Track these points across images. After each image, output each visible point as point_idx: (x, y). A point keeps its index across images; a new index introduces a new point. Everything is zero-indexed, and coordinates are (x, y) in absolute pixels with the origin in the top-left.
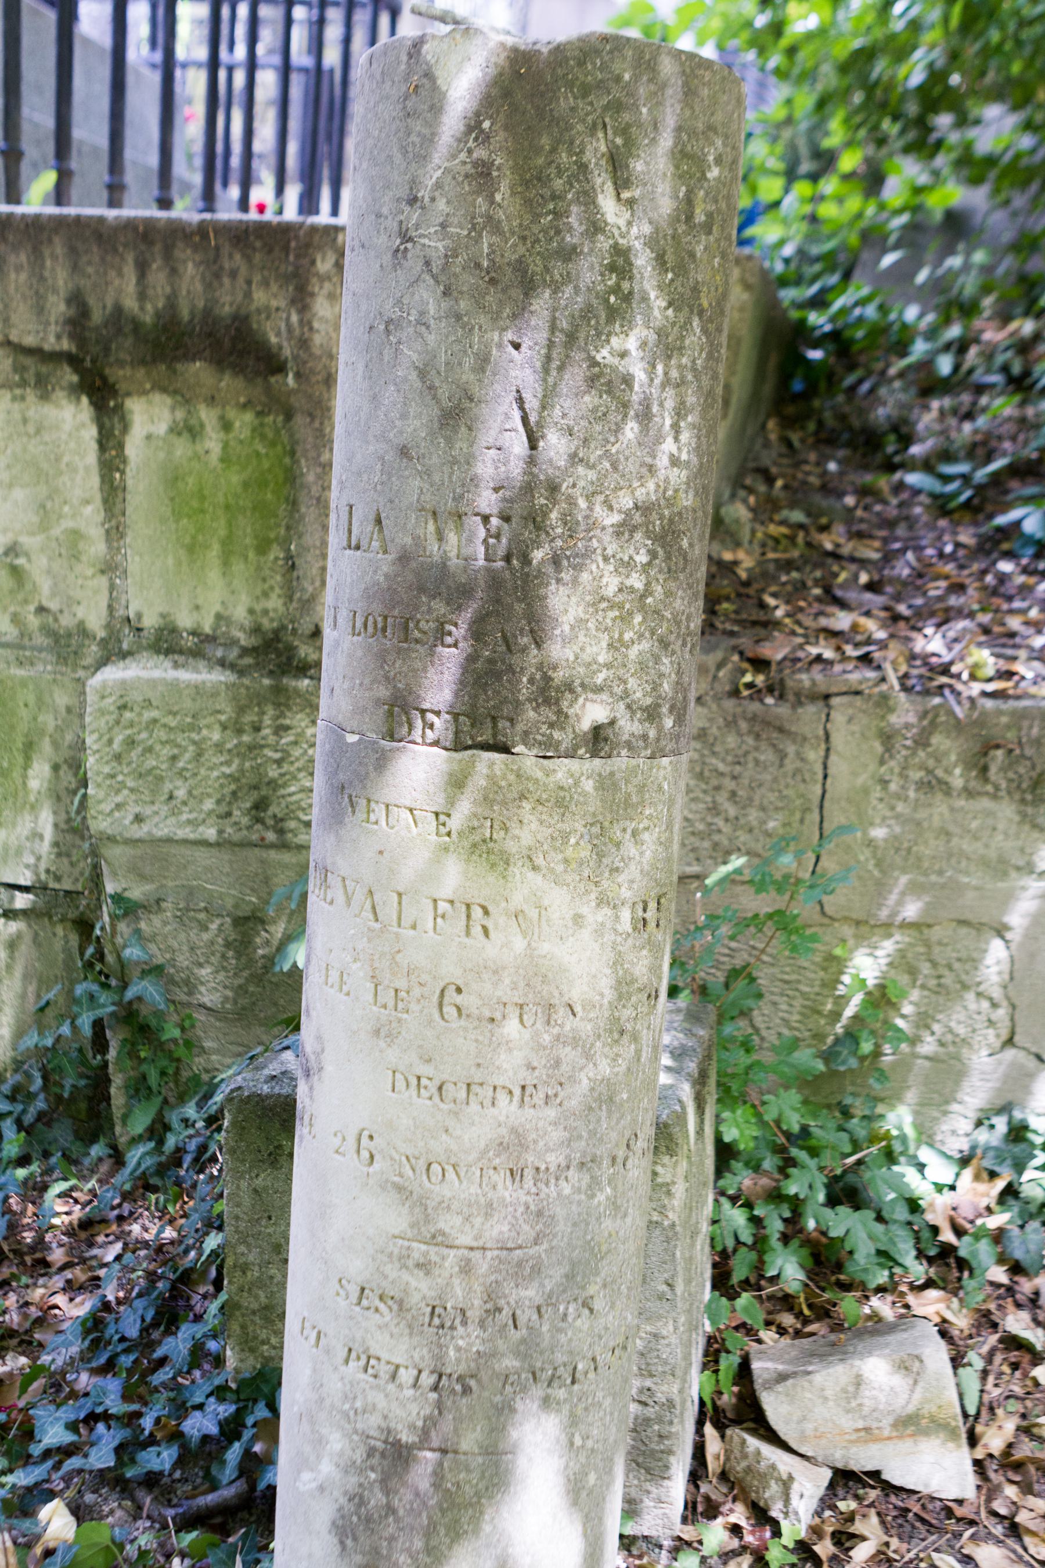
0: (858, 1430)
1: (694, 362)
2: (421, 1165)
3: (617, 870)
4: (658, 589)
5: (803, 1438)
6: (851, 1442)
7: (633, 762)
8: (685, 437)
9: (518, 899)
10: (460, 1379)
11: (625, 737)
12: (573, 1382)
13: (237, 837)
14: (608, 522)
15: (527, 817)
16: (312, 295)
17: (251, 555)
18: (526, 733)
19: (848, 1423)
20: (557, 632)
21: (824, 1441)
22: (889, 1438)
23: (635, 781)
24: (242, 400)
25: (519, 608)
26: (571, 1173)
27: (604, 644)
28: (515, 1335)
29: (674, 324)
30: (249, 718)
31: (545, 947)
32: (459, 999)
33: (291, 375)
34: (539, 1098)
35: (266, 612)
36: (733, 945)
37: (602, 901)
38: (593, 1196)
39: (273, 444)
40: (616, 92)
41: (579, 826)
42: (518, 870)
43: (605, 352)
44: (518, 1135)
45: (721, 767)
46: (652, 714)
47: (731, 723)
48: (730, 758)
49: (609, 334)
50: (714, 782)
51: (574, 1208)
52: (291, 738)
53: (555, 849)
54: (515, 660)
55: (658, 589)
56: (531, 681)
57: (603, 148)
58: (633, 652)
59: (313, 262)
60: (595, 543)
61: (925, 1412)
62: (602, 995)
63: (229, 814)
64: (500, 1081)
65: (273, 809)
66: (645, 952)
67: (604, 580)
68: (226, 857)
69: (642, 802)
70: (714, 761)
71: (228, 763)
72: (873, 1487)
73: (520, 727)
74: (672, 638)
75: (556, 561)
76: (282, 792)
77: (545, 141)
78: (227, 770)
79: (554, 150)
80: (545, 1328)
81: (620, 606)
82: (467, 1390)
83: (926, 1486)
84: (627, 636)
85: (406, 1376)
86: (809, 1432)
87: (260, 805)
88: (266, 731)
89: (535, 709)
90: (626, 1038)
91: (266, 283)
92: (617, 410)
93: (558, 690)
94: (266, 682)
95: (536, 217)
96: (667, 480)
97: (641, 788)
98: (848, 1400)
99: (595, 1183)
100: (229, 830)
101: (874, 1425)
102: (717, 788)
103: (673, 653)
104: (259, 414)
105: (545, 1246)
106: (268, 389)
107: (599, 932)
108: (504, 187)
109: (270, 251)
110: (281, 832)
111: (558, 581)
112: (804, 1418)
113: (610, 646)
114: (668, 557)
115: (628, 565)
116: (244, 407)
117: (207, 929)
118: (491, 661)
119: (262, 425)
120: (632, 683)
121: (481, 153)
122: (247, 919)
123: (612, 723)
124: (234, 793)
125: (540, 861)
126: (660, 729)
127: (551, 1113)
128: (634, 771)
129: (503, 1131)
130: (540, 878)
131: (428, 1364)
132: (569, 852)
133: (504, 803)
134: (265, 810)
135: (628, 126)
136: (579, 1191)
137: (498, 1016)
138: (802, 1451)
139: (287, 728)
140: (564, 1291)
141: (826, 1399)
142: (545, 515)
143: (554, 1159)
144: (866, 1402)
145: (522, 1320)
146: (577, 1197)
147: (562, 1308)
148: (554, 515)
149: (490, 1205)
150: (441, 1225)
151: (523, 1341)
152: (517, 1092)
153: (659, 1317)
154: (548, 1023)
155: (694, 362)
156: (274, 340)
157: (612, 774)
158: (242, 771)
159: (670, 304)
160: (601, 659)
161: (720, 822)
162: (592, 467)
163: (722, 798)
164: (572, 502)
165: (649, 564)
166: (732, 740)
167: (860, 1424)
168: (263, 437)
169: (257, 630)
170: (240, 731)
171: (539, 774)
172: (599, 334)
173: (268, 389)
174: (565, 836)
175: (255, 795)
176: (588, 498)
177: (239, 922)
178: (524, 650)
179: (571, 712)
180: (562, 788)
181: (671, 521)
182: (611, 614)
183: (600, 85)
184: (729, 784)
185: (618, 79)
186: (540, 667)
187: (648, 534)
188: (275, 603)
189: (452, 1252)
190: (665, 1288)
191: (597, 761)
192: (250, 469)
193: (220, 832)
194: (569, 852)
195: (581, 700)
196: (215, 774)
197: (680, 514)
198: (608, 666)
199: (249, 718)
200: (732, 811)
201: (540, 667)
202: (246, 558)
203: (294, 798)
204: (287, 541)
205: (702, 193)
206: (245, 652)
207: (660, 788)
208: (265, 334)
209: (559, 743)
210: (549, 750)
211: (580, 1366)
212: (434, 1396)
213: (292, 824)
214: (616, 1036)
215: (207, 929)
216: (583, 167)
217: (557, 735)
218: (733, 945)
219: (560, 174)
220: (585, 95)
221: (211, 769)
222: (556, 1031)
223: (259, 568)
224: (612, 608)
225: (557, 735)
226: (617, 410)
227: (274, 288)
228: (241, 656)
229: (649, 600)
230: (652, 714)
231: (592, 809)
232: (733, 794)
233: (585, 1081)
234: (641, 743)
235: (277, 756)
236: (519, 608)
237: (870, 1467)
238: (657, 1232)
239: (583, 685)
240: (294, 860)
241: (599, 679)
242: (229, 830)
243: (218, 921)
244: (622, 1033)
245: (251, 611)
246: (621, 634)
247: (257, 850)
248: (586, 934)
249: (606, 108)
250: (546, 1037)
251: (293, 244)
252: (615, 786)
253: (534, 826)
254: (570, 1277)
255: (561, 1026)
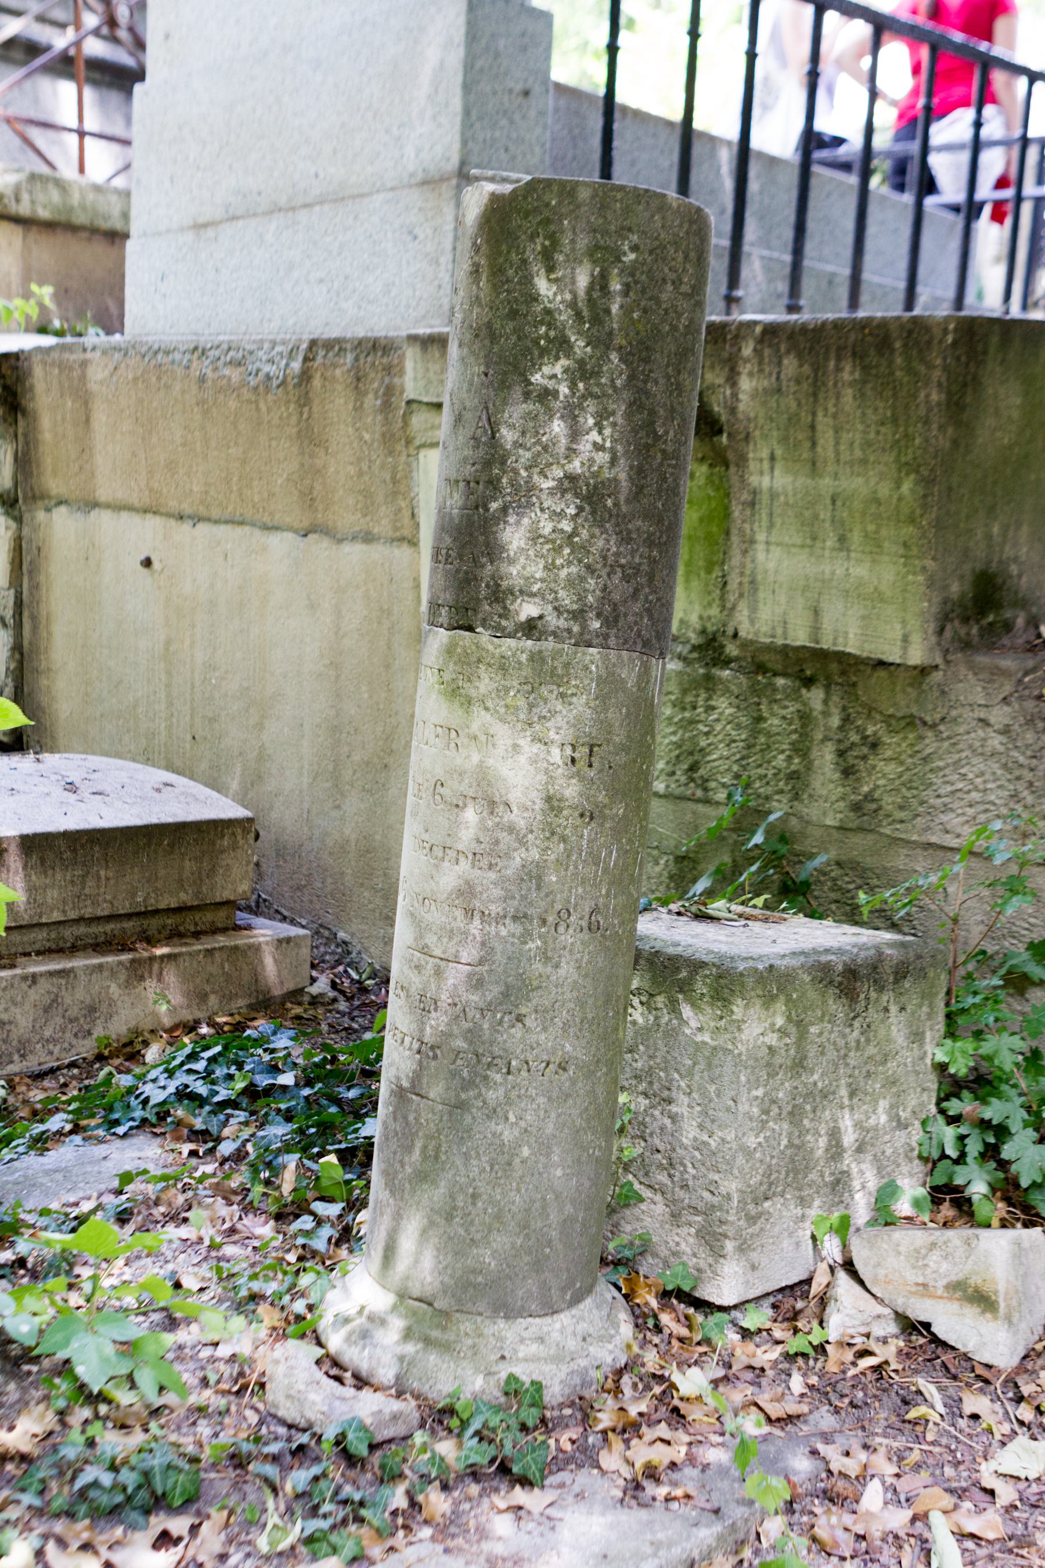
0: (917, 1284)
1: (613, 381)
2: (421, 898)
3: (545, 717)
4: (585, 533)
5: (876, 1280)
6: (911, 1292)
7: (560, 646)
8: (607, 432)
9: (475, 727)
10: (432, 1048)
11: (552, 628)
12: (509, 1073)
13: (678, 792)
14: (544, 486)
15: (483, 675)
16: (739, 374)
17: (702, 574)
18: (484, 620)
19: (912, 1276)
20: (505, 555)
21: (891, 1287)
22: (941, 1297)
23: (561, 660)
24: (700, 455)
25: (481, 538)
26: (507, 921)
27: (541, 566)
28: (466, 1025)
29: (591, 357)
30: (689, 699)
31: (491, 762)
32: (442, 790)
33: (725, 435)
34: (484, 863)
35: (709, 618)
36: (1032, 920)
37: (537, 739)
38: (526, 943)
39: (718, 489)
40: (546, 213)
41: (515, 683)
42: (477, 709)
43: (538, 376)
44: (470, 887)
45: (1021, 759)
46: (578, 615)
47: (1030, 722)
48: (1029, 753)
49: (541, 365)
50: (1017, 773)
51: (509, 946)
52: (715, 716)
53: (499, 697)
54: (478, 572)
55: (585, 533)
56: (487, 586)
57: (539, 248)
58: (563, 573)
59: (740, 349)
60: (534, 499)
61: (972, 1282)
62: (534, 803)
63: (673, 773)
64: (460, 847)
65: (702, 772)
66: (574, 781)
67: (541, 524)
68: (671, 807)
69: (568, 674)
70: (1015, 754)
71: (674, 733)
72: (924, 1336)
73: (480, 616)
74: (599, 566)
75: (504, 509)
76: (709, 758)
77: (504, 247)
78: (674, 739)
79: (509, 252)
80: (486, 1026)
81: (553, 541)
82: (435, 1057)
83: (964, 1345)
84: (559, 562)
85: (407, 1040)
86: (881, 1277)
87: (693, 768)
88: (700, 710)
89: (490, 605)
90: (556, 838)
91: (712, 367)
92: (545, 413)
93: (504, 592)
94: (702, 671)
95: (498, 296)
96: (592, 461)
97: (567, 665)
98: (917, 1259)
99: (526, 937)
100: (673, 786)
101: (931, 1283)
102: (1018, 778)
103: (599, 577)
104: (711, 466)
105: (486, 968)
106: (713, 447)
107: (533, 761)
108: (484, 278)
109: (716, 342)
110: (706, 790)
111: (505, 522)
112: (878, 1265)
113: (545, 567)
114: (593, 512)
115: (561, 515)
116: (702, 459)
117: (658, 864)
118: (466, 573)
119: (712, 474)
120: (562, 594)
121: (476, 259)
122: (684, 858)
123: (541, 617)
124: (678, 757)
125: (489, 704)
126: (584, 627)
127: (492, 875)
128: (559, 652)
129: (462, 882)
130: (489, 716)
131: (416, 1034)
132: (509, 700)
133: (469, 664)
134: (696, 771)
135: (554, 233)
136: (513, 936)
137: (461, 804)
138: (874, 1291)
139: (713, 708)
140: (501, 1004)
141: (899, 1253)
142: (499, 480)
143: (495, 909)
144: (931, 1264)
145: (470, 1015)
146: (511, 939)
147: (499, 1016)
148: (504, 480)
149: (452, 931)
150: (427, 941)
151: (470, 1031)
152: (470, 856)
153: (727, 1126)
154: (492, 813)
155: (613, 381)
156: (716, 409)
157: (540, 652)
158: (682, 740)
159: (588, 345)
160: (538, 576)
161: (1019, 808)
162: (529, 449)
163: (1021, 786)
164: (516, 472)
165: (577, 515)
166: (1030, 737)
167: (920, 1280)
168: (712, 482)
169: (703, 632)
170: (684, 709)
171: (490, 647)
172: (534, 365)
173: (713, 447)
174: (507, 690)
175: (691, 760)
176: (527, 468)
177: (680, 859)
178: (483, 566)
179: (512, 608)
180: (503, 657)
181: (595, 487)
182: (547, 547)
183: (536, 210)
184: (1028, 776)
185: (548, 205)
186: (493, 577)
187: (577, 495)
188: (714, 611)
189: (431, 960)
190: (731, 1103)
191: (530, 642)
192: (704, 507)
193: (668, 787)
194: (509, 700)
195: (519, 601)
196: (667, 741)
197: (602, 483)
198: (542, 580)
199: (689, 699)
200: (1030, 799)
201: (493, 577)
202: (699, 575)
203: (716, 764)
204: (723, 563)
205: (616, 271)
206: (695, 648)
207: (586, 668)
208: (711, 405)
209: (505, 628)
210: (501, 633)
211: (514, 1063)
212: (418, 1056)
213: (712, 784)
214: (547, 834)
215: (658, 864)
216: (524, 262)
217: (504, 623)
218: (1032, 920)
219: (511, 267)
220: (526, 217)
221: (664, 737)
222: (497, 820)
223: (707, 585)
224: (547, 542)
225: (504, 623)
226: (545, 413)
227: (718, 369)
228: (691, 652)
229: (576, 539)
230: (578, 615)
231: (524, 674)
232: (1031, 784)
233: (518, 859)
234: (565, 634)
235: (706, 729)
236: (481, 538)
237: (922, 1318)
238: (730, 1058)
239: (521, 592)
240: (714, 813)
241: (535, 588)
242: (673, 786)
243: (665, 858)
244: (553, 833)
245: (701, 618)
246: (553, 561)
247: (690, 804)
248: (522, 759)
249: (540, 223)
250: (490, 823)
251: (729, 337)
252: (543, 661)
253: (487, 681)
254: (506, 995)
255: (501, 817)
